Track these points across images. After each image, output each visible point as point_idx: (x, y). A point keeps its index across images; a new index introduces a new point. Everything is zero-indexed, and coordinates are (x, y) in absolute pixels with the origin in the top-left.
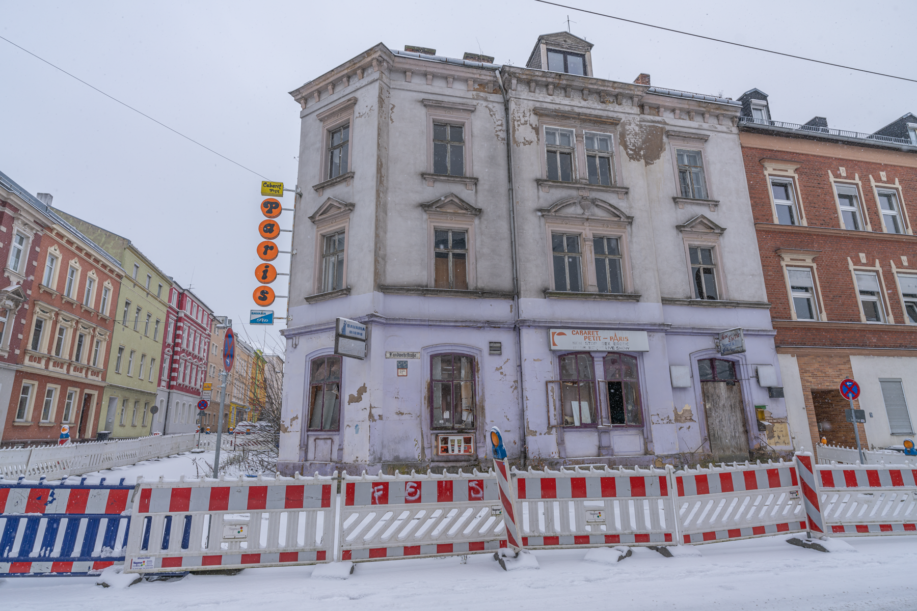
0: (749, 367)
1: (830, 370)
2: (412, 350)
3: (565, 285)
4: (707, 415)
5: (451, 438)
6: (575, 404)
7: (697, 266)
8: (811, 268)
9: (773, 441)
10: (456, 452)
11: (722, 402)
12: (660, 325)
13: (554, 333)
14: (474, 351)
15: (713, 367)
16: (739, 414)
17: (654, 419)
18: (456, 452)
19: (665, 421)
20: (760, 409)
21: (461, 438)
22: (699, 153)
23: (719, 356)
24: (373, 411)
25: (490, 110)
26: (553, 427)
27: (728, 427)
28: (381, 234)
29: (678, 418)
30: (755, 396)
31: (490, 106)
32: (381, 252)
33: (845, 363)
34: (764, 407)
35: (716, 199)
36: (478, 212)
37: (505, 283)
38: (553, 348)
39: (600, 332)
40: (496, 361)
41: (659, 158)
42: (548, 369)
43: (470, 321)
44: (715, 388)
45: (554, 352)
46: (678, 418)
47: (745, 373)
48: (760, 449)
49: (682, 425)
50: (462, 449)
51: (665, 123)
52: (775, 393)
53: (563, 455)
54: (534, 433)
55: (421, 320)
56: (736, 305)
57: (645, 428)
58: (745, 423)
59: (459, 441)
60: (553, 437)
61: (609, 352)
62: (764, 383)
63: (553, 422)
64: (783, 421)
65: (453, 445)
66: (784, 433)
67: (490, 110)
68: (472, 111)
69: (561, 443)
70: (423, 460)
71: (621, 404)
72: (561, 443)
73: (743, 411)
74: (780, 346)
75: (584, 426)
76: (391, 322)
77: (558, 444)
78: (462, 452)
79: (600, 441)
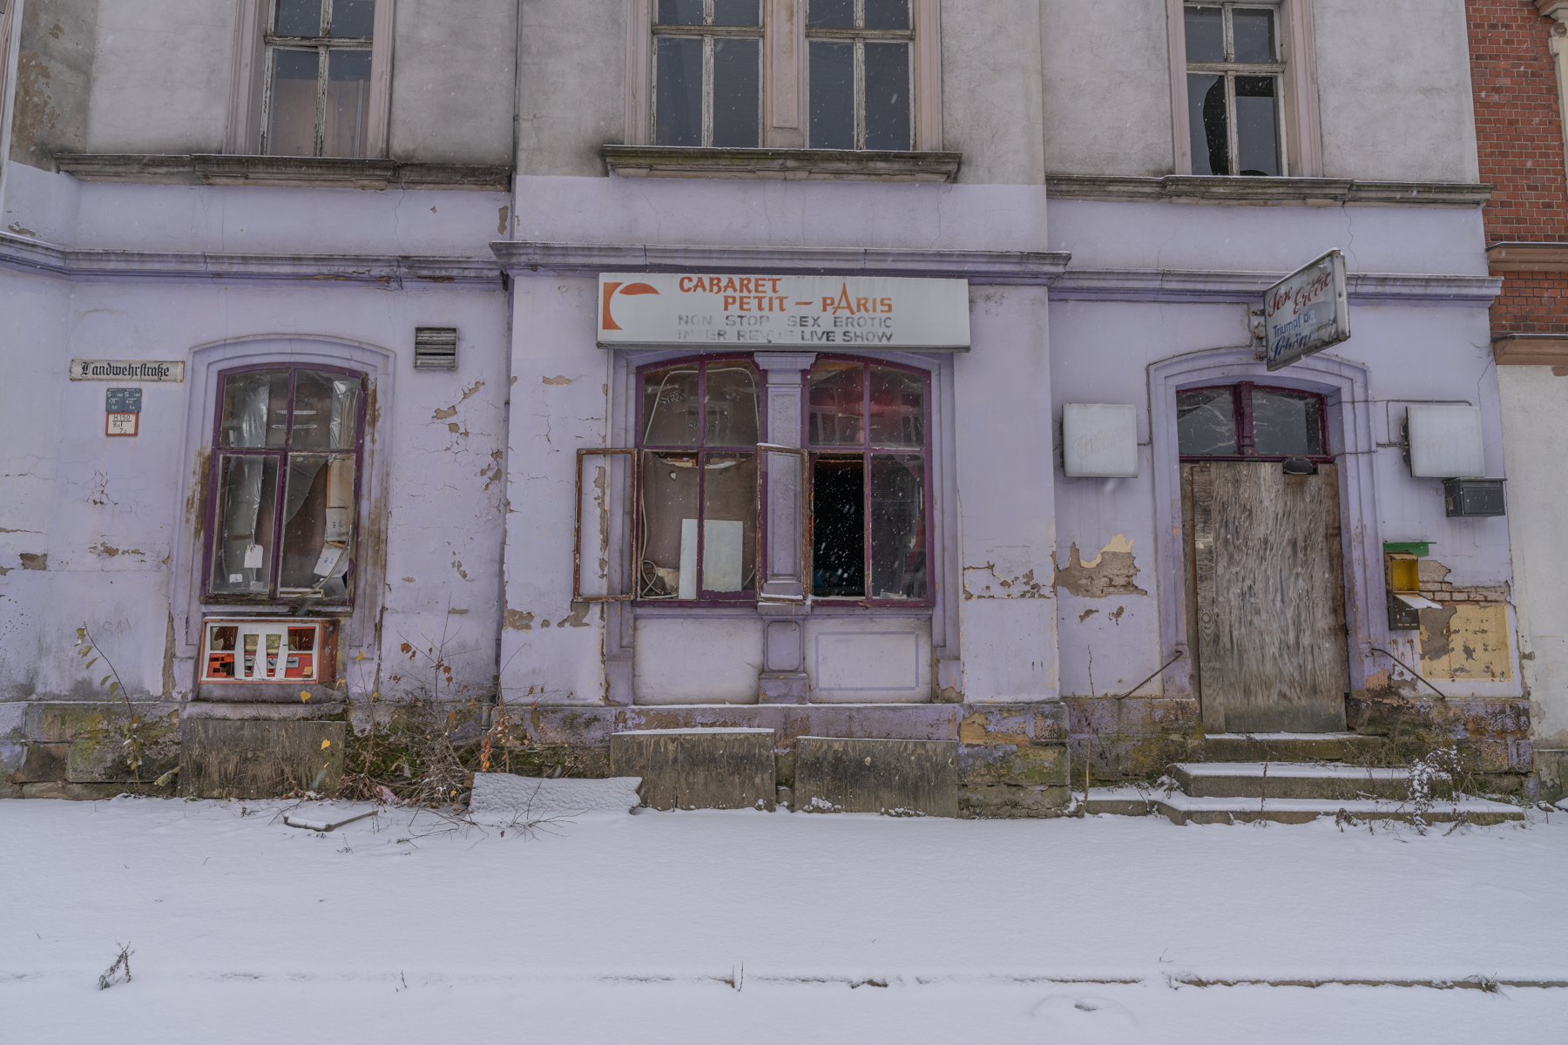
0: (1378, 412)
2: (154, 355)
3: (692, 128)
4: (1195, 570)
5: (244, 629)
6: (689, 526)
7: (1212, 69)
9: (1443, 663)
10: (260, 674)
11: (1260, 531)
12: (1025, 257)
13: (610, 289)
14: (367, 358)
15: (1240, 415)
16: (1322, 573)
17: (975, 581)
18: (260, 674)
19: (1017, 589)
20: (1403, 557)
21: (281, 630)
23: (1261, 372)
26: (588, 601)
27: (1275, 614)
29: (1069, 578)
30: (1383, 507)
32: (66, 44)
34: (1421, 547)
37: (486, 141)
38: (606, 336)
39: (787, 284)
40: (437, 389)
42: (597, 410)
43: (344, 258)
44: (1237, 483)
45: (618, 352)
46: (1069, 578)
47: (1355, 430)
48: (1390, 690)
49: (1090, 603)
50: (281, 664)
53: (621, 692)
54: (523, 620)
55: (179, 257)
56: (1348, 193)
57: (937, 613)
58: (1341, 602)
59: (272, 641)
60: (591, 635)
61: (823, 356)
63: (594, 584)
64: (1492, 596)
65: (250, 653)
66: (1491, 638)
69: (620, 655)
70: (167, 697)
71: (863, 528)
72: (620, 655)
73: (1338, 561)
74: (1507, 341)
75: (709, 600)
77: (606, 658)
78: (280, 676)
79: (765, 652)
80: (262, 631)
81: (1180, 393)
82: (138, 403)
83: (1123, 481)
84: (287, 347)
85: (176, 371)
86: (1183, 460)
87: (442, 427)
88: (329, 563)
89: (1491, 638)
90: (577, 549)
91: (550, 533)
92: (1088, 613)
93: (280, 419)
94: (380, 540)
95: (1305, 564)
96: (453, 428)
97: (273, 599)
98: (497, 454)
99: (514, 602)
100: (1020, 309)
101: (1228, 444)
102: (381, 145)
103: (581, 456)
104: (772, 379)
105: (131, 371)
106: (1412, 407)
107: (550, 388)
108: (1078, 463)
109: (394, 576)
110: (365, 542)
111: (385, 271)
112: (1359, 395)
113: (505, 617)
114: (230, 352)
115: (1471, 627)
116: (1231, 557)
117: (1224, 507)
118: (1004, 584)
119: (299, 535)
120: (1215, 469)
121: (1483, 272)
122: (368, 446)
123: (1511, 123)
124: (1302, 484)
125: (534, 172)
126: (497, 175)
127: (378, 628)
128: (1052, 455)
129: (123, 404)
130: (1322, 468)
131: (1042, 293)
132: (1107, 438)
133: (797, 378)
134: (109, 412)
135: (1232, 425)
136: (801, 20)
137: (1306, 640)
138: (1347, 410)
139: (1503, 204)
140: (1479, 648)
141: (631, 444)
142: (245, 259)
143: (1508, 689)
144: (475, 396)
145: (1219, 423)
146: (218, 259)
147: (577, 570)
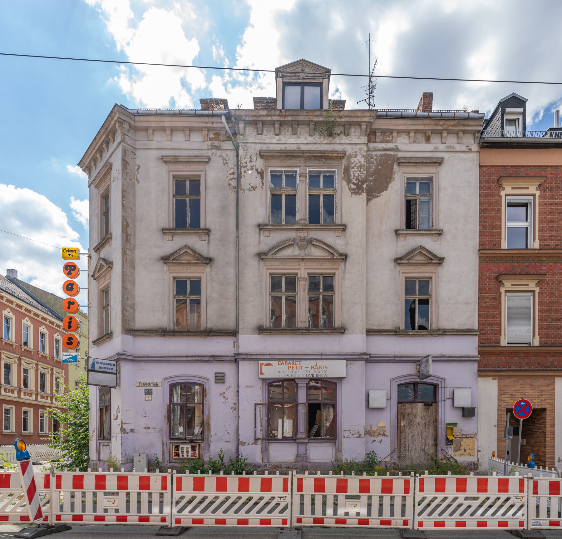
1: (530, 392)
4: (400, 431)
5: (181, 446)
6: (280, 421)
7: (411, 298)
8: (533, 292)
9: (458, 453)
10: (185, 456)
11: (418, 420)
14: (202, 380)
17: (346, 434)
18: (185, 456)
19: (355, 436)
20: (450, 427)
21: (189, 446)
22: (431, 179)
23: (418, 380)
24: (124, 426)
25: (224, 159)
28: (129, 286)
29: (368, 433)
30: (447, 414)
31: (224, 155)
32: (129, 302)
33: (548, 385)
34: (455, 424)
35: (441, 227)
36: (209, 261)
41: (385, 188)
43: (198, 356)
44: (412, 408)
46: (368, 433)
49: (374, 439)
50: (190, 454)
51: (397, 149)
52: (468, 412)
54: (244, 444)
55: (160, 357)
56: (443, 332)
57: (337, 441)
58: (436, 439)
59: (187, 448)
60: (259, 447)
62: (456, 404)
64: (472, 436)
65: (183, 452)
67: (224, 159)
68: (207, 162)
72: (265, 451)
73: (436, 428)
76: (136, 359)
79: (298, 451)
80: (185, 446)
81: (399, 385)
82: (152, 392)
83: (381, 409)
84: (185, 378)
85: (160, 384)
86: (399, 403)
87: (222, 397)
88: (197, 430)
89: (471, 447)
90: (255, 427)
91: (250, 423)
92: (374, 441)
93: (183, 395)
94: (209, 425)
95: (428, 429)
96: (224, 397)
97: (185, 439)
98: (235, 404)
99: (241, 439)
100: (358, 366)
101: (411, 399)
102: (205, 326)
103: (256, 405)
104: (299, 385)
105: (150, 384)
106: (455, 389)
107: (248, 388)
108: (372, 405)
109: (212, 433)
110: (205, 425)
111: (208, 359)
112: (443, 386)
113: (239, 443)
114: (172, 379)
115: (466, 444)
116: (410, 427)
117: (409, 414)
118: (353, 434)
119: (189, 425)
120: (407, 405)
121: (476, 353)
122: (205, 402)
123: (488, 312)
124: (428, 409)
125: (243, 334)
126: (234, 333)
127: (209, 446)
128: (365, 405)
129: (148, 392)
130: (434, 404)
131: (364, 362)
132: (379, 398)
133: (305, 385)
134: (145, 394)
135: (413, 393)
136: (307, 290)
137: (427, 448)
138: (440, 389)
139: (484, 334)
140: (468, 449)
141: (267, 402)
142: (175, 357)
143: (473, 459)
144: (229, 390)
145: (410, 393)
146: (169, 357)
147: (255, 432)
